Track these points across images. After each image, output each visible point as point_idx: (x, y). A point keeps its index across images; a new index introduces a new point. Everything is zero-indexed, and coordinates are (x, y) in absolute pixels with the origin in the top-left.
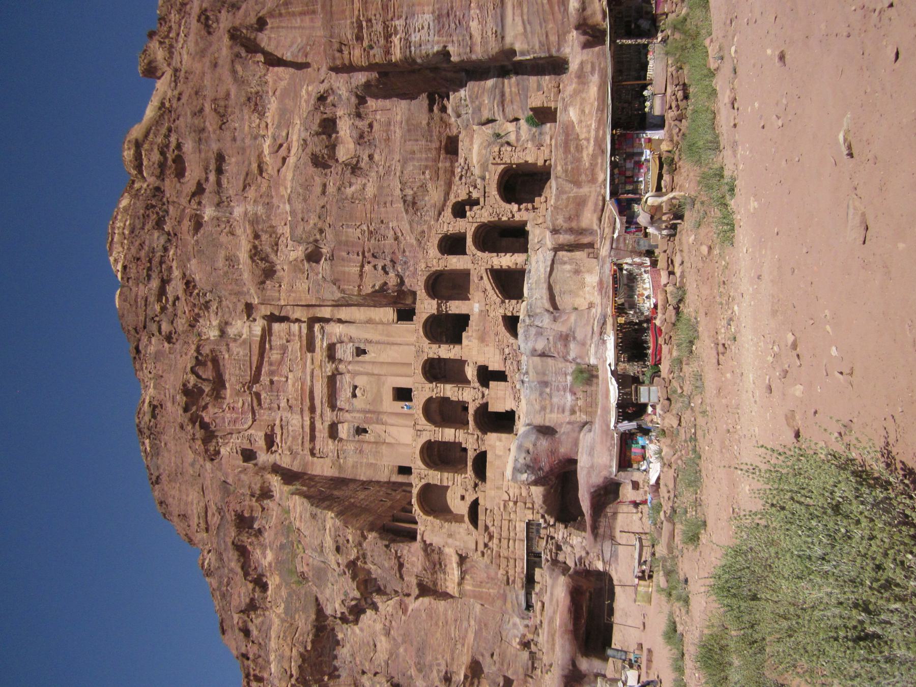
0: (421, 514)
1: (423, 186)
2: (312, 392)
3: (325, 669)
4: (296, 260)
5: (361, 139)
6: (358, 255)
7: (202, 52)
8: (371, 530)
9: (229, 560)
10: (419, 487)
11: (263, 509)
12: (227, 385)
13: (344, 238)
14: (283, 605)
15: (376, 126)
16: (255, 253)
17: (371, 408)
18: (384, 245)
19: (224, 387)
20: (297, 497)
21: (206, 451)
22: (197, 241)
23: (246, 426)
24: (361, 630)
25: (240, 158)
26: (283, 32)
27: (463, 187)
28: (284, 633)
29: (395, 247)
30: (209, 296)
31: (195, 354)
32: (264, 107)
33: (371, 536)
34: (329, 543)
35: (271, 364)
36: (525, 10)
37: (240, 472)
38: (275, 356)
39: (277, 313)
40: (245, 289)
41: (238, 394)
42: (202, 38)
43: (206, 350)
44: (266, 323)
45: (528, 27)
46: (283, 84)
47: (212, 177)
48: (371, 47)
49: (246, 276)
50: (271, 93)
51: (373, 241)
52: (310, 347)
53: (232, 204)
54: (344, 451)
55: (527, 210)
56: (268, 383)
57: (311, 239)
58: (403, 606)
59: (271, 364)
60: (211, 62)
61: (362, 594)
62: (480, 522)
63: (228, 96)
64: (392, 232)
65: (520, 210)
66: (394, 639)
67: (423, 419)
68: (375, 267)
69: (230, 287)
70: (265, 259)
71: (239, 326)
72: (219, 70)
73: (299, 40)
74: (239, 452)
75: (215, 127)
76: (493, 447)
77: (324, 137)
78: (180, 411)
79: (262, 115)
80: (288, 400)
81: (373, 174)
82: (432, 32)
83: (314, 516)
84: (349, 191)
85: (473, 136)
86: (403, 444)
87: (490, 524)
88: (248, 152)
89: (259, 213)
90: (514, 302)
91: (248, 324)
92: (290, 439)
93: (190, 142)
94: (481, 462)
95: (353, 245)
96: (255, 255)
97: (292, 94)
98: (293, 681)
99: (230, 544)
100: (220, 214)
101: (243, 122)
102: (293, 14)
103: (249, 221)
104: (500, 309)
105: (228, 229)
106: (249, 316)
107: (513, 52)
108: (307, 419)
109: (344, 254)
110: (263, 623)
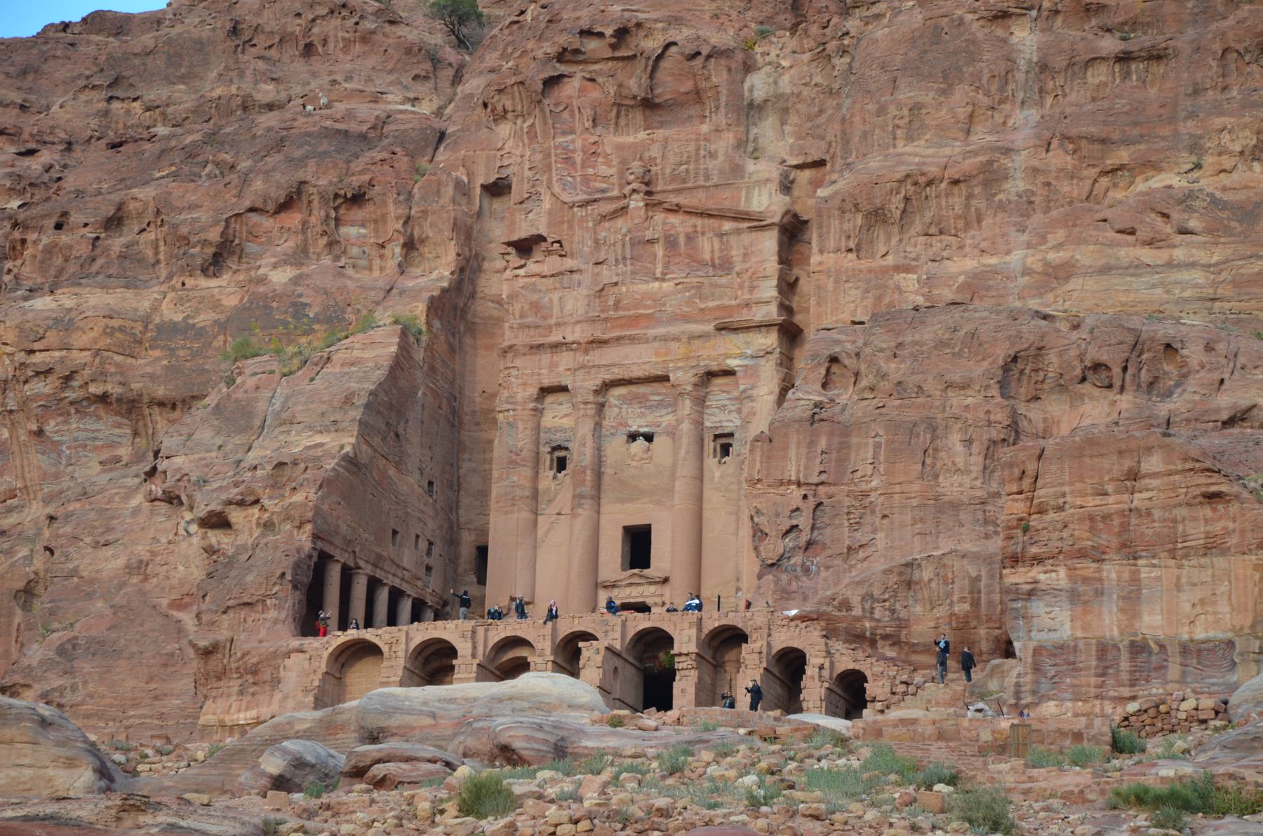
2: (633, 339)
3: (52, 423)
8: (316, 537)
9: (268, 173)
10: (376, 641)
13: (855, 440)
14: (178, 317)
16: (920, 185)
17: (606, 479)
18: (841, 525)
20: (394, 349)
22: (961, 21)
23: (557, 188)
24: (136, 512)
27: (887, 689)
28: (121, 329)
30: (841, 63)
33: (304, 539)
35: (690, 238)
37: (458, 184)
43: (718, 75)
44: (777, 219)
48: (1026, 530)
51: (847, 501)
56: (649, 235)
58: (187, 599)
66: (122, 585)
67: (497, 639)
68: (797, 509)
69: (857, 119)
71: (777, 142)
80: (616, 284)
82: (1044, 636)
84: (955, 440)
86: (535, 555)
88: (1166, 131)
89: (1007, 185)
95: (842, 461)
96: (916, 184)
98: (21, 357)
99: (300, 175)
100: (1020, 76)
103: (990, 162)
105: (985, 101)
106: (797, 167)
108: (576, 334)
109: (823, 443)
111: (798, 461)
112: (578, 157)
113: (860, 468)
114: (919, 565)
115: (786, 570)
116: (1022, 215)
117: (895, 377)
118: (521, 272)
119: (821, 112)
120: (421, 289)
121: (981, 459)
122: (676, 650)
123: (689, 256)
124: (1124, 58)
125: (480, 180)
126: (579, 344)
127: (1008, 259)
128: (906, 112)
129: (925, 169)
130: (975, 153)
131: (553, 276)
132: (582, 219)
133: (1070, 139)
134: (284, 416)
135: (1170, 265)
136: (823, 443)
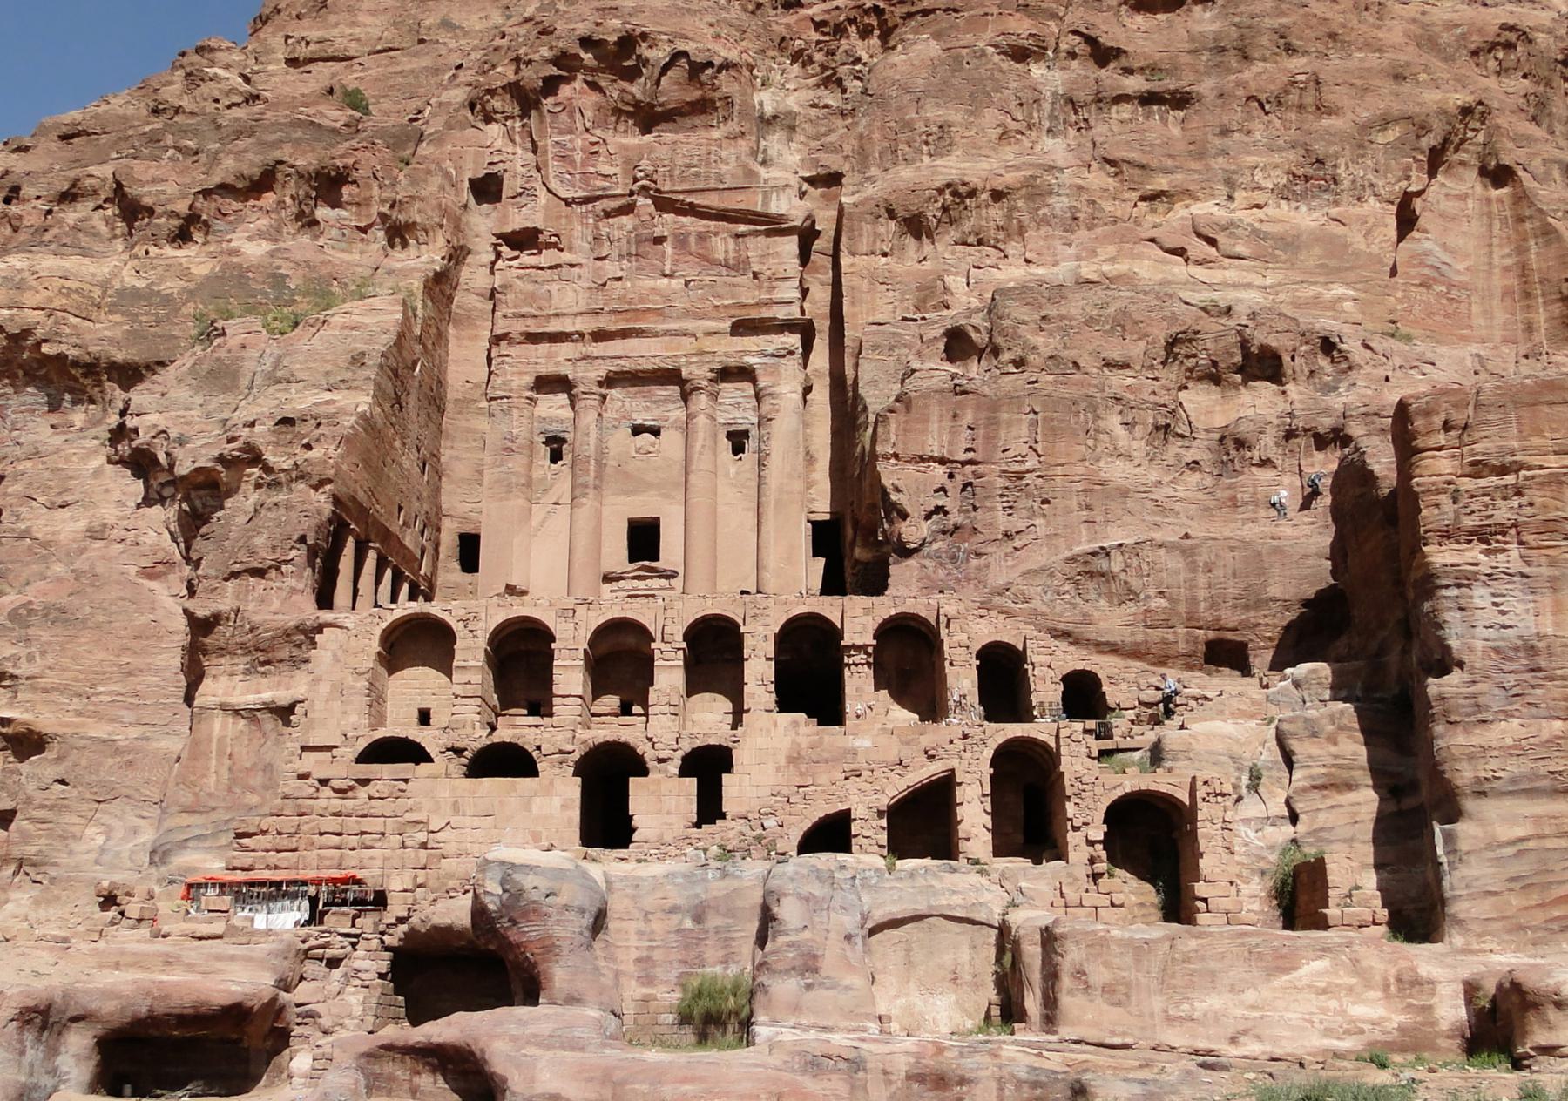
0: (384, 625)
1: (1131, 594)
4: (946, 290)
5: (1234, 443)
6: (968, 450)
7: (1430, 39)
8: (336, 500)
11: (364, 230)
12: (648, 138)
13: (1005, 416)
15: (1264, 475)
16: (960, 194)
18: (993, 509)
19: (646, 130)
20: (399, 316)
21: (492, 92)
22: (983, 54)
23: (554, 184)
25: (1181, 147)
26: (1477, 227)
29: (988, 535)
31: (717, 61)
32: (1302, 197)
33: (321, 502)
34: (301, 401)
36: (1549, 844)
37: (447, 175)
38: (722, 245)
39: (817, 245)
40: (874, 171)
41: (632, 165)
42: (1463, 37)
45: (1510, 851)
46: (1357, 241)
47: (1134, 84)
49: (905, 175)
50: (1334, 212)
51: (1001, 482)
52: (743, 327)
53: (1072, 132)
54: (507, 412)
55: (1092, 861)
56: (658, 232)
57: (999, 340)
59: (702, 237)
60: (1408, 64)
61: (183, 478)
62: (376, 767)
63: (1322, 109)
64: (1021, 526)
65: (1091, 843)
67: (601, 621)
68: (943, 489)
69: (876, 136)
70: (949, 216)
72: (1387, 86)
73: (1461, 267)
74: (494, 169)
75: (1253, 85)
76: (548, 791)
77: (1238, 358)
78: (582, 29)
79: (1283, 194)
80: (620, 279)
81: (1154, 476)
83: (358, 360)
84: (1113, 422)
85: (1252, 716)
87: (371, 789)
88: (1194, 165)
89: (1052, 200)
90: (883, 838)
91: (794, 181)
92: (530, 287)
93: (1215, 27)
94: (505, 761)
95: (990, 439)
96: (955, 193)
97: (1333, 263)
100: (1047, 106)
101: (1264, 154)
102: (1521, 250)
103: (1034, 177)
104: (867, 805)
105: (1013, 126)
106: (811, 181)
107: (1453, 815)
109: (968, 418)
110: (96, 235)
111: (940, 436)
112: (578, 157)
113: (1013, 447)
114: (1108, 554)
115: (928, 556)
116: (1066, 231)
117: (1047, 352)
118: (515, 263)
119: (831, 131)
120: (414, 269)
121: (1143, 443)
122: (846, 641)
123: (699, 256)
124: (1148, 99)
125: (469, 175)
126: (582, 335)
127: (1055, 269)
128: (935, 129)
129: (966, 179)
130: (1017, 168)
131: (550, 268)
132: (583, 216)
133: (1111, 163)
134: (279, 374)
135: (1226, 285)
136: (968, 418)
